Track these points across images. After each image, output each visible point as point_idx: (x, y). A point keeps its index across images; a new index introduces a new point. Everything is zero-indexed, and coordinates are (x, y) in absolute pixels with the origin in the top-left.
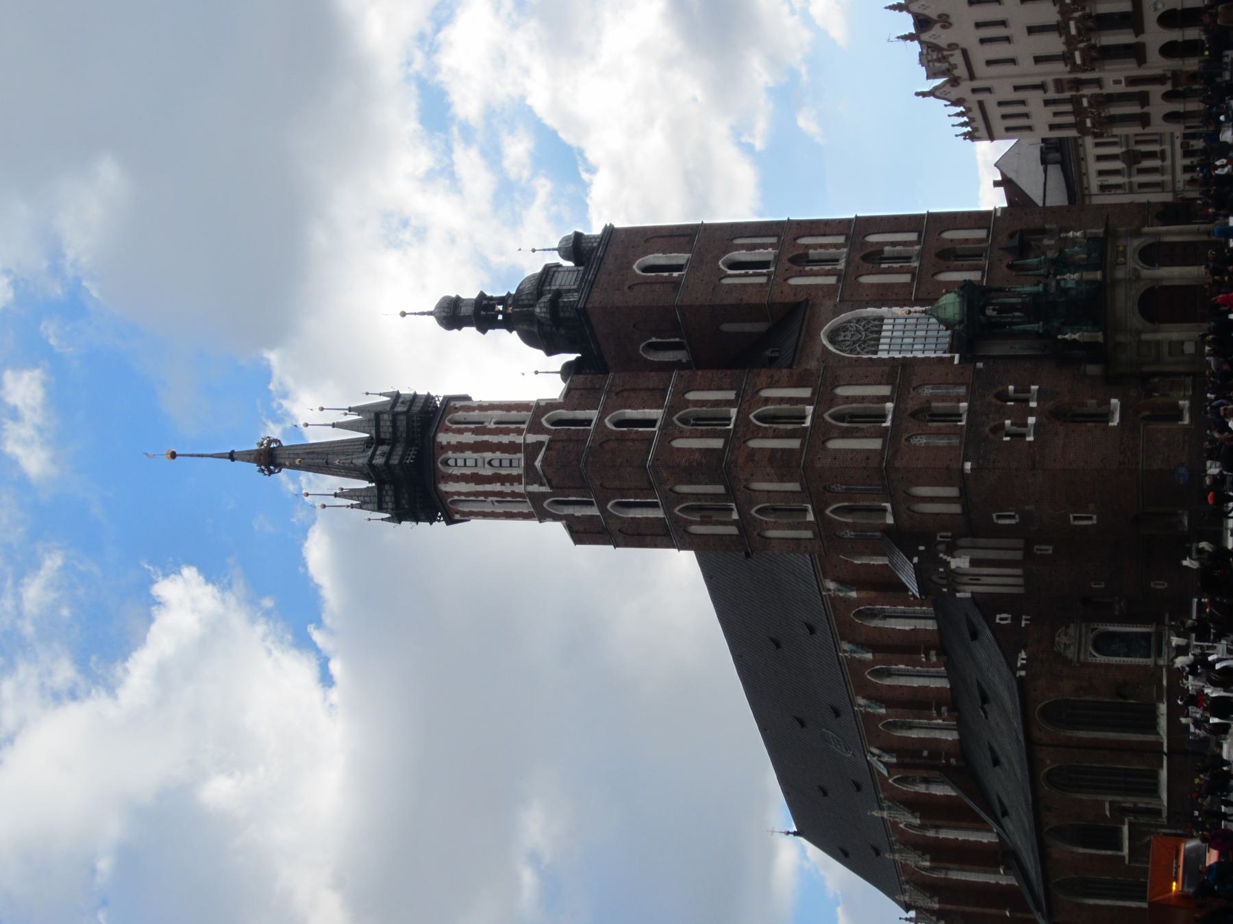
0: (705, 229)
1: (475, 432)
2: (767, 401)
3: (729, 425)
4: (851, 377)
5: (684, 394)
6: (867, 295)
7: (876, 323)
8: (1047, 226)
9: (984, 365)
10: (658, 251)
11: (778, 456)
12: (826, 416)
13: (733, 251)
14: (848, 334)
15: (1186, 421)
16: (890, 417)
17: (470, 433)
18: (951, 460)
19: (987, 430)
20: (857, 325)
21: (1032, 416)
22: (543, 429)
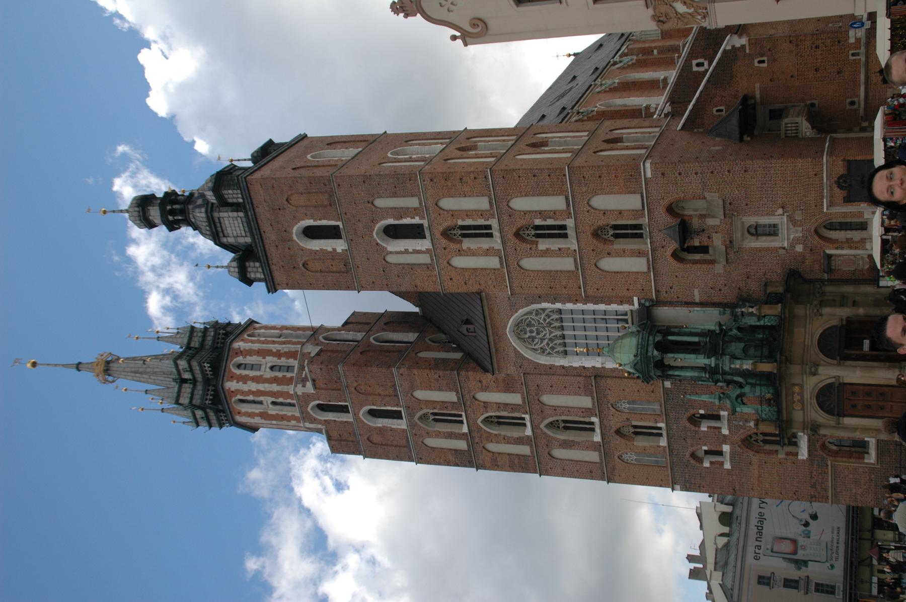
0: (339, 185)
2: (486, 405)
3: (461, 422)
4: (551, 386)
5: (412, 395)
6: (536, 288)
7: (555, 316)
8: (707, 195)
9: (671, 384)
10: (306, 216)
11: (516, 461)
12: (542, 426)
13: (381, 220)
14: (534, 329)
15: (872, 457)
16: (598, 430)
17: (260, 418)
18: (662, 480)
19: (688, 455)
21: (726, 444)
22: (315, 419)
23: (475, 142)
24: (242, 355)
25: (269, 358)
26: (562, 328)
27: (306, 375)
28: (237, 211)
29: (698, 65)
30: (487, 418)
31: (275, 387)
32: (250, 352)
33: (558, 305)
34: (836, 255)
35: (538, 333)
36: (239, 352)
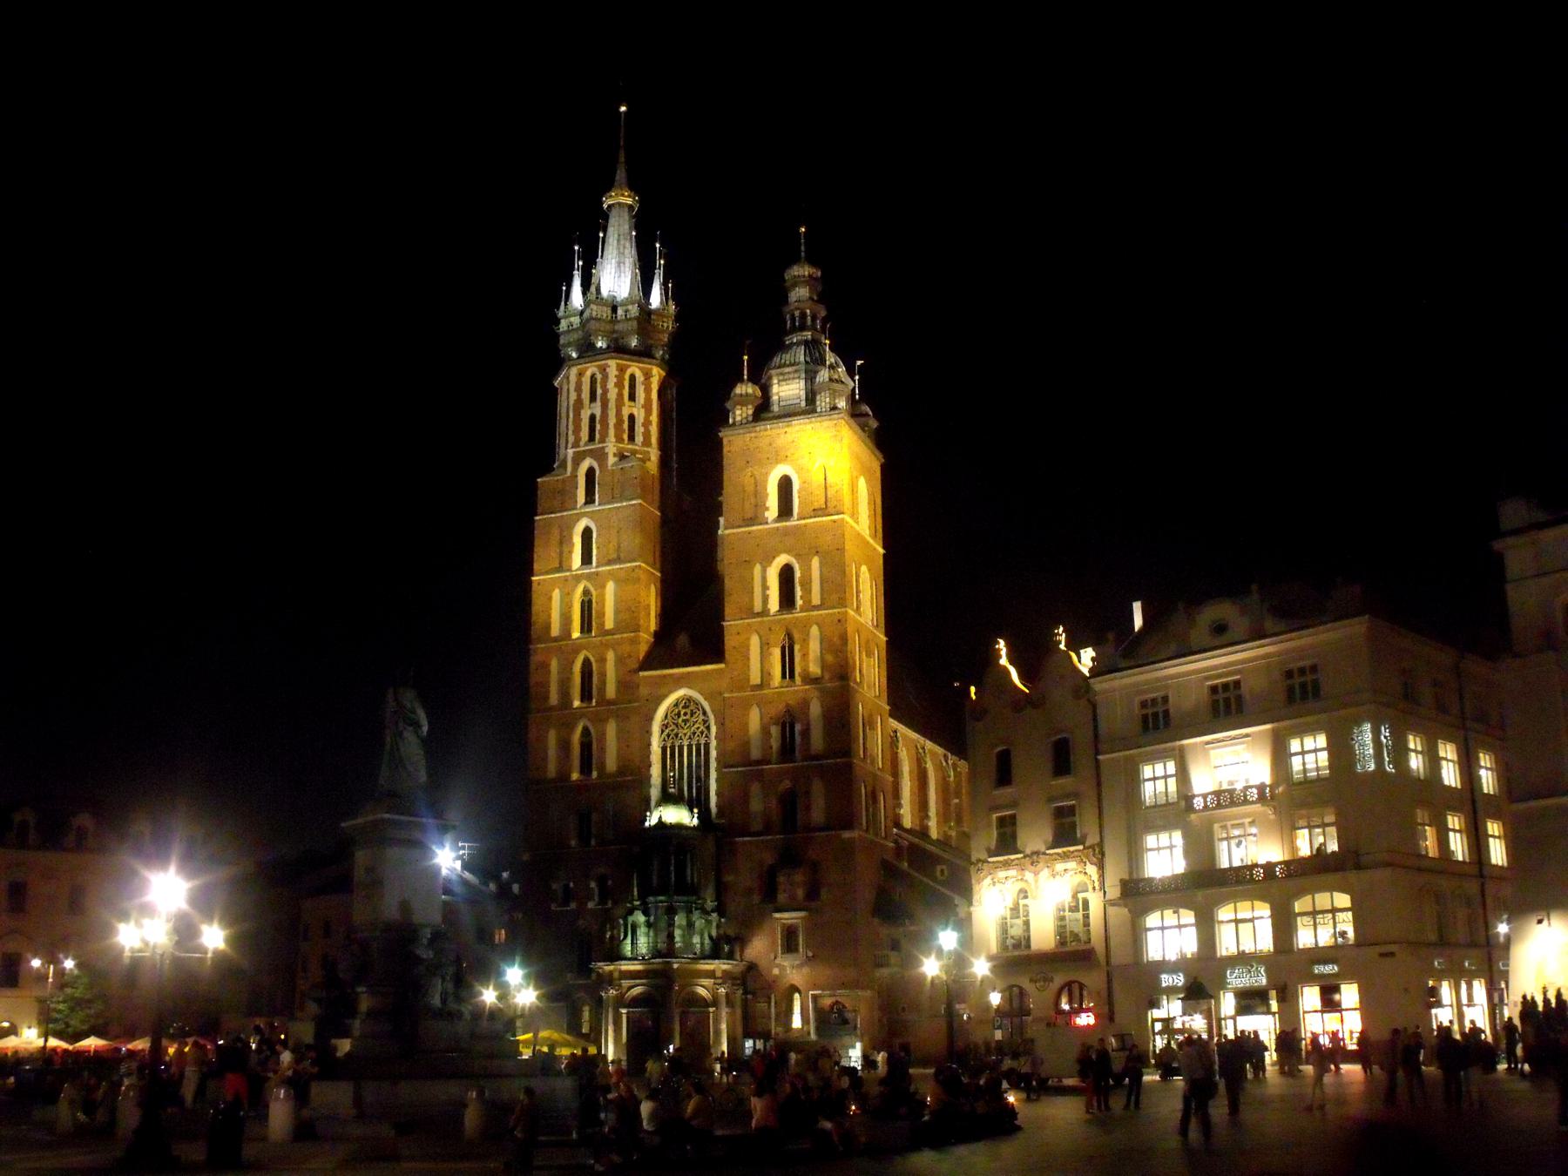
0: (835, 522)
1: (579, 402)
2: (603, 660)
13: (798, 563)
17: (575, 398)
20: (700, 720)
23: (874, 654)
24: (646, 379)
25: (642, 412)
26: (690, 746)
27: (627, 457)
28: (807, 399)
29: (942, 871)
30: (589, 660)
31: (612, 421)
32: (648, 390)
33: (713, 743)
34: (769, 1003)
35: (683, 721)
36: (648, 376)
